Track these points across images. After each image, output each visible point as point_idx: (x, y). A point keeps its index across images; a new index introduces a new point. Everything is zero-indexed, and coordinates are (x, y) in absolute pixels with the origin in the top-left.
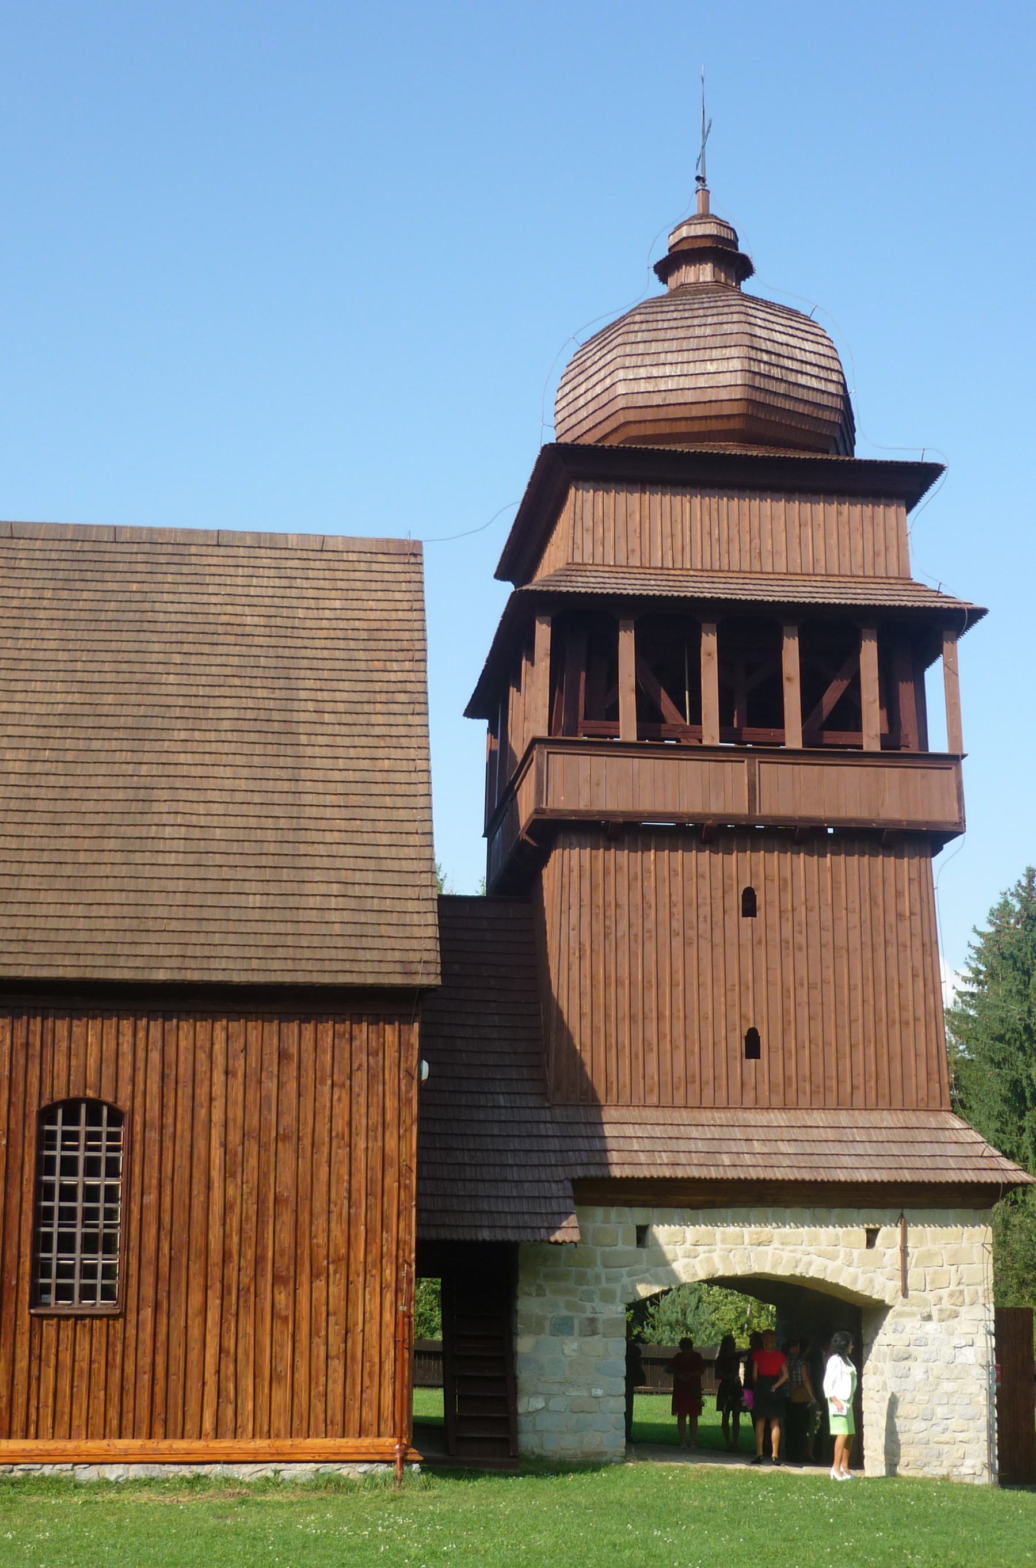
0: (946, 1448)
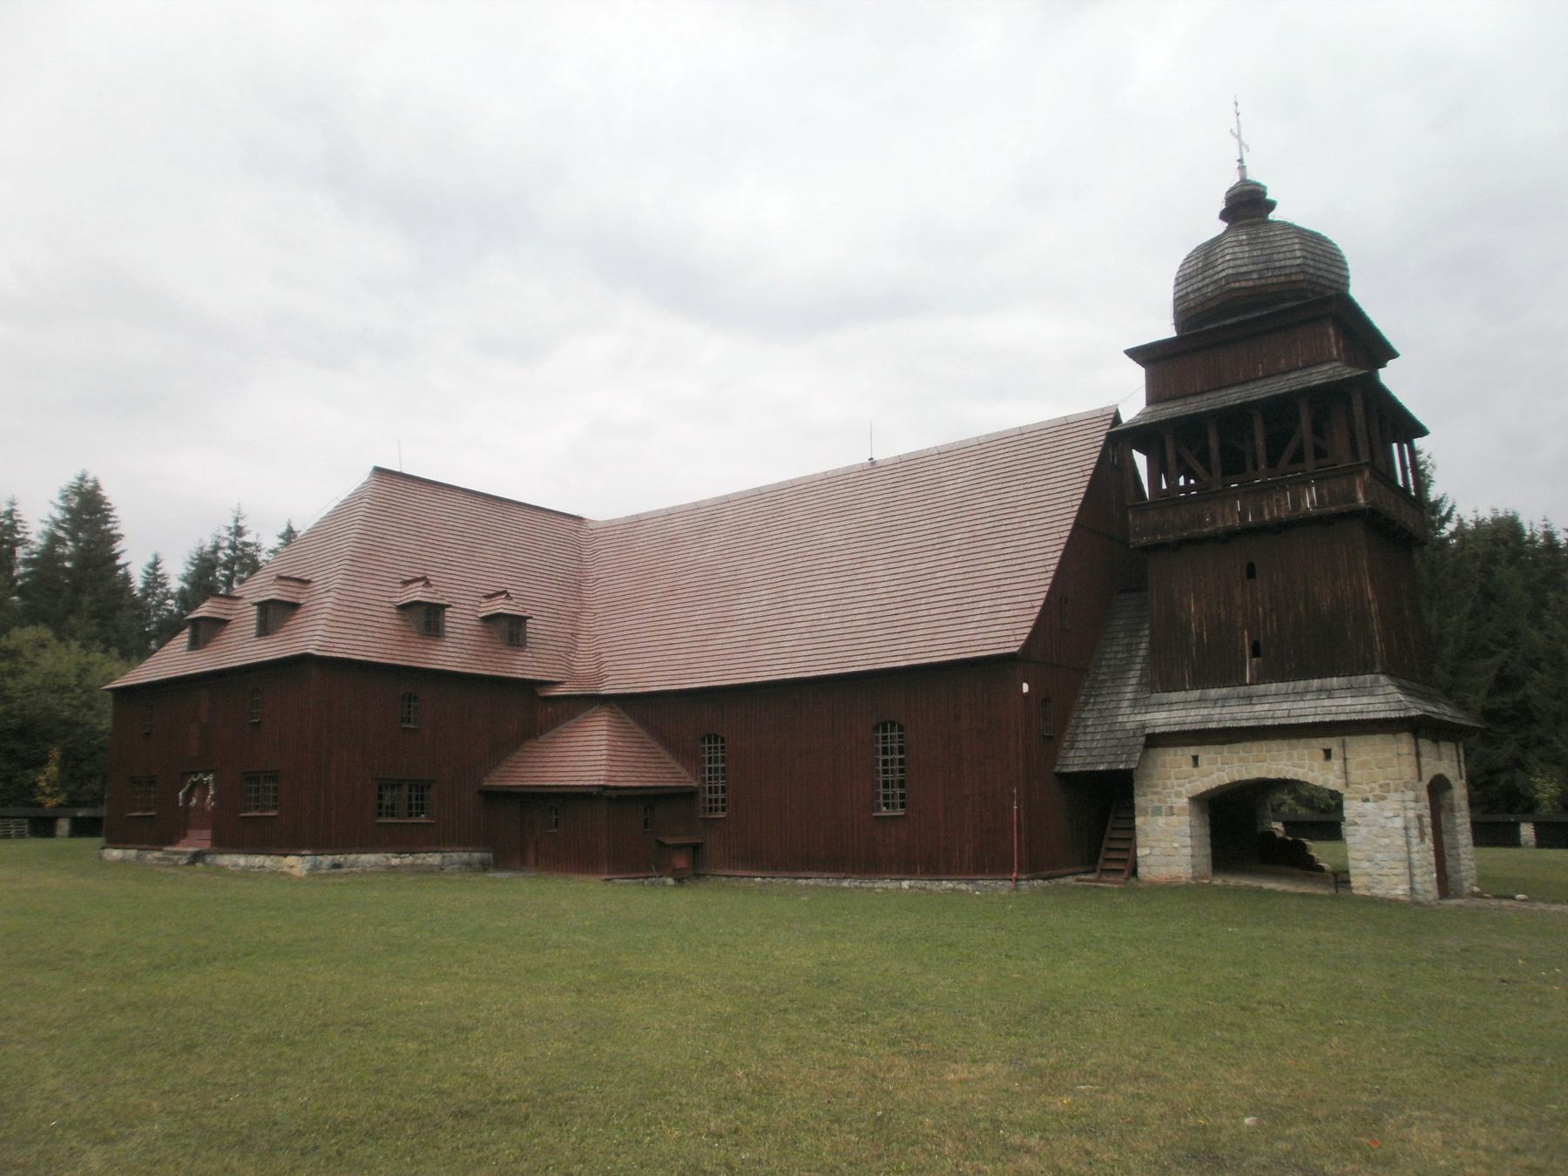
0: (1385, 878)
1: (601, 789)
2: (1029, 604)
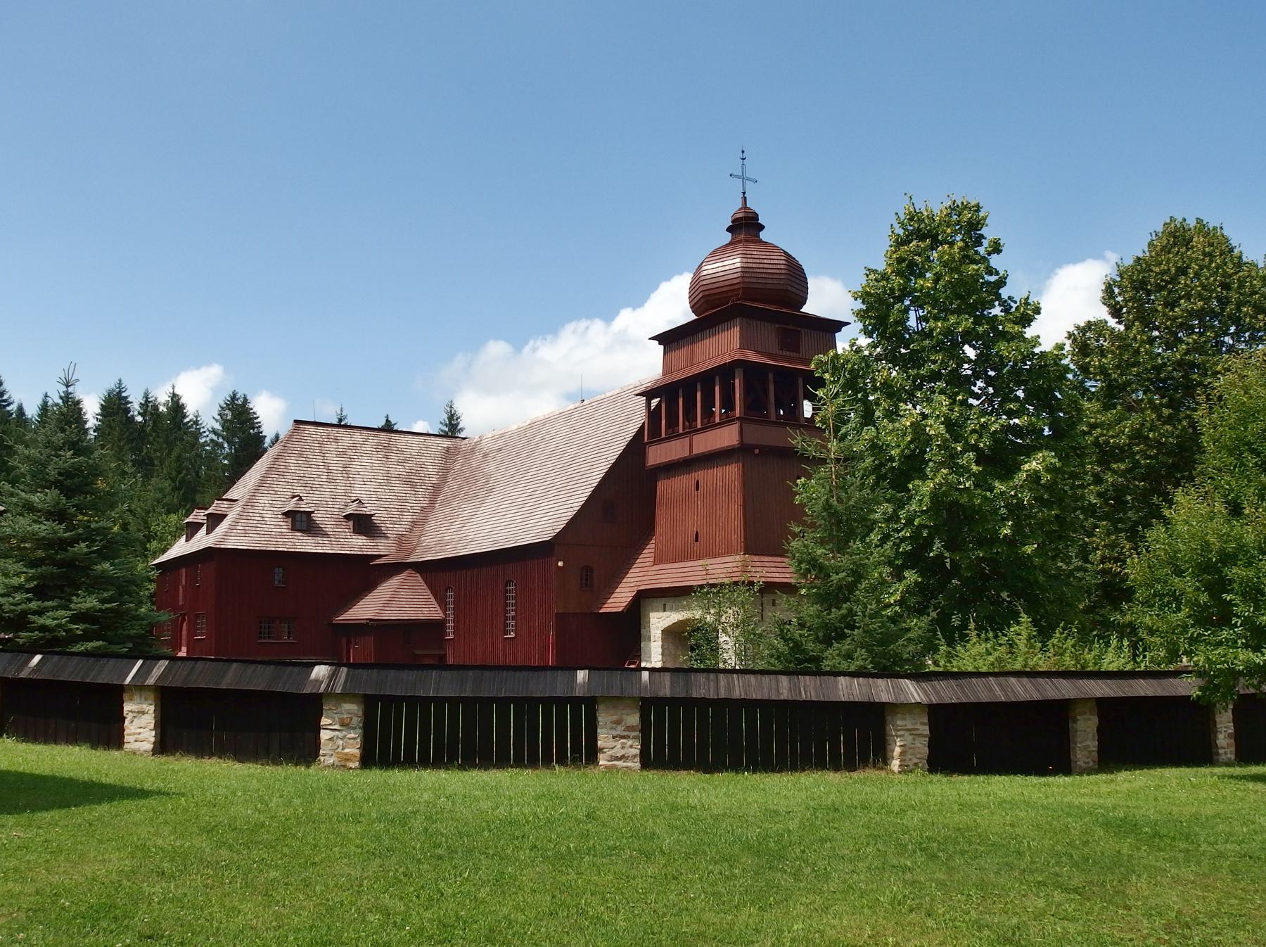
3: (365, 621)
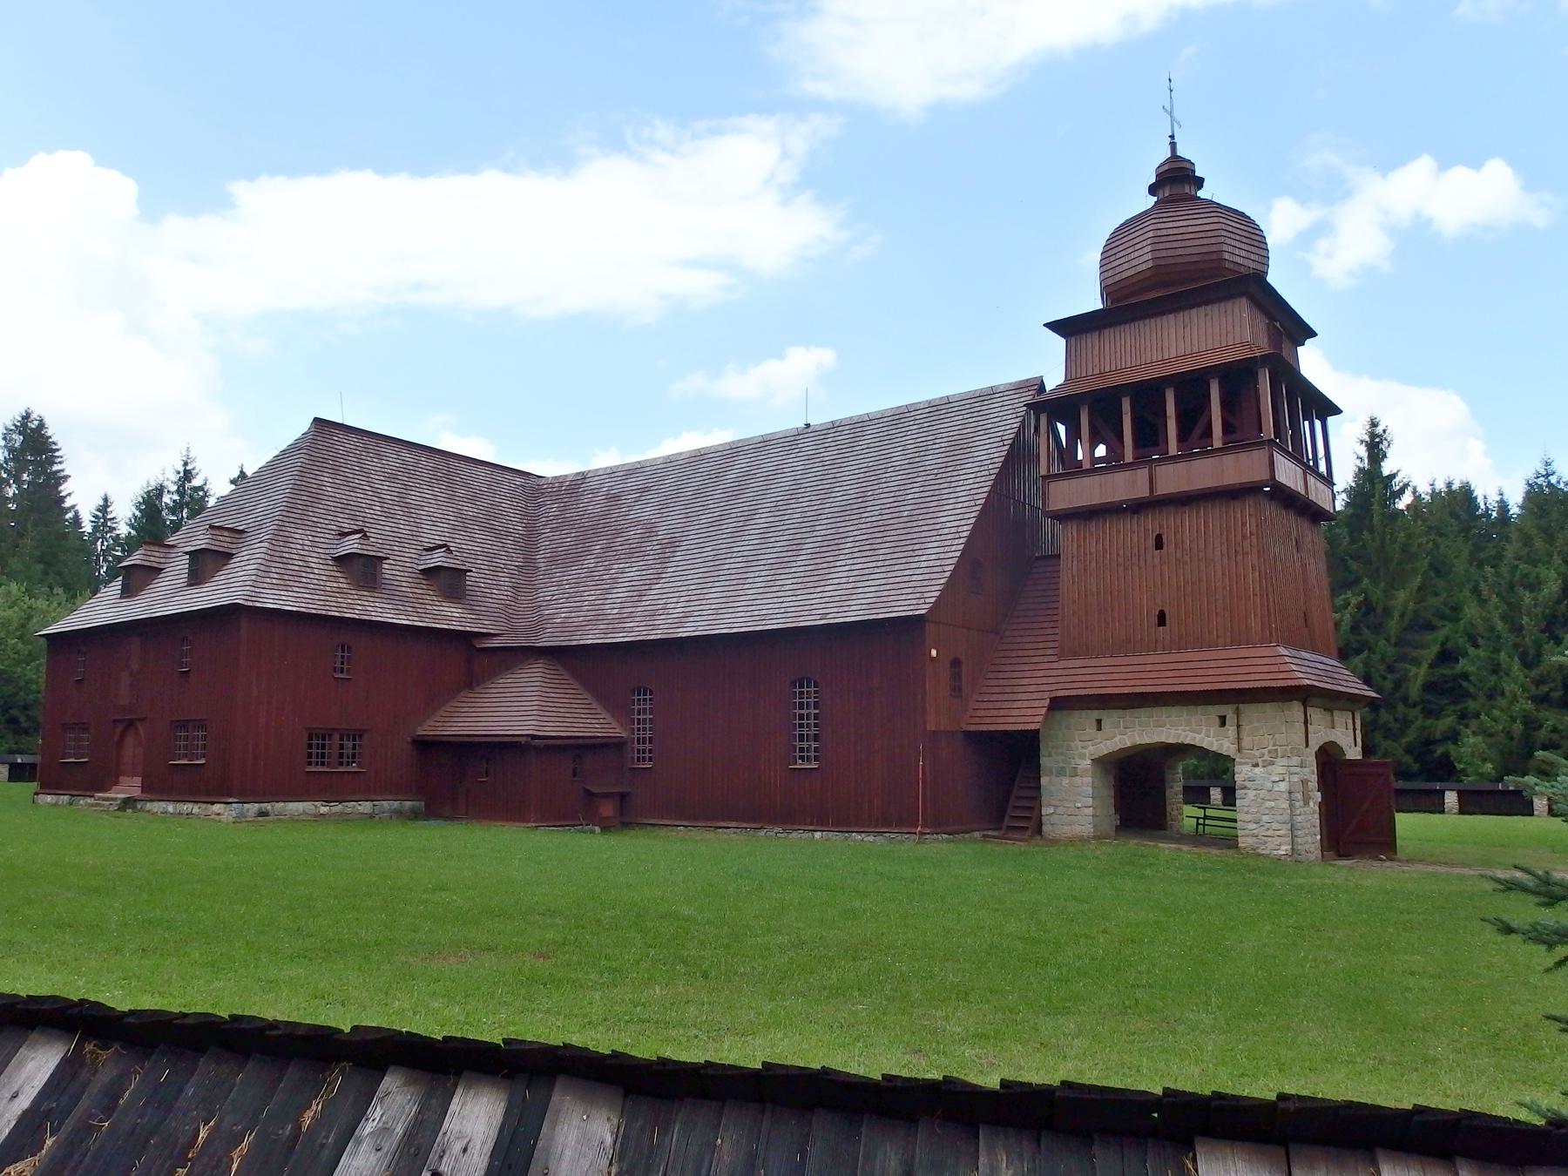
0: (1270, 839)
1: (529, 739)
2: (940, 569)
3: (524, 739)
